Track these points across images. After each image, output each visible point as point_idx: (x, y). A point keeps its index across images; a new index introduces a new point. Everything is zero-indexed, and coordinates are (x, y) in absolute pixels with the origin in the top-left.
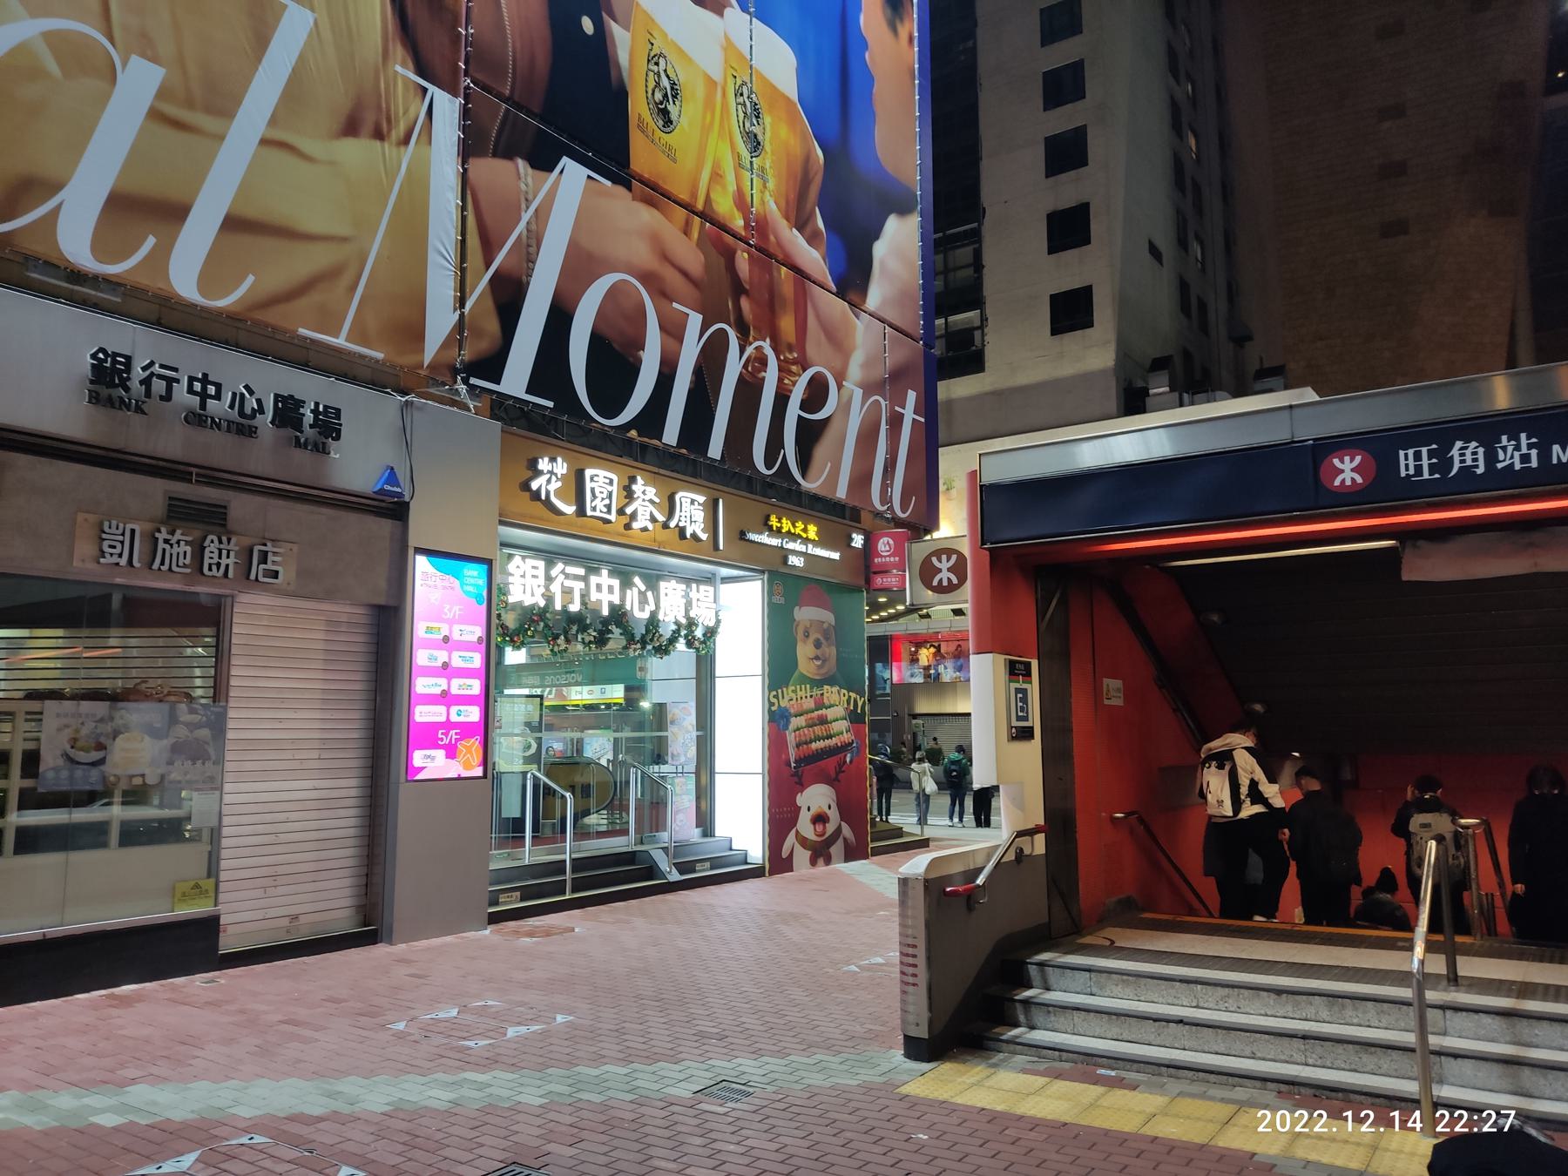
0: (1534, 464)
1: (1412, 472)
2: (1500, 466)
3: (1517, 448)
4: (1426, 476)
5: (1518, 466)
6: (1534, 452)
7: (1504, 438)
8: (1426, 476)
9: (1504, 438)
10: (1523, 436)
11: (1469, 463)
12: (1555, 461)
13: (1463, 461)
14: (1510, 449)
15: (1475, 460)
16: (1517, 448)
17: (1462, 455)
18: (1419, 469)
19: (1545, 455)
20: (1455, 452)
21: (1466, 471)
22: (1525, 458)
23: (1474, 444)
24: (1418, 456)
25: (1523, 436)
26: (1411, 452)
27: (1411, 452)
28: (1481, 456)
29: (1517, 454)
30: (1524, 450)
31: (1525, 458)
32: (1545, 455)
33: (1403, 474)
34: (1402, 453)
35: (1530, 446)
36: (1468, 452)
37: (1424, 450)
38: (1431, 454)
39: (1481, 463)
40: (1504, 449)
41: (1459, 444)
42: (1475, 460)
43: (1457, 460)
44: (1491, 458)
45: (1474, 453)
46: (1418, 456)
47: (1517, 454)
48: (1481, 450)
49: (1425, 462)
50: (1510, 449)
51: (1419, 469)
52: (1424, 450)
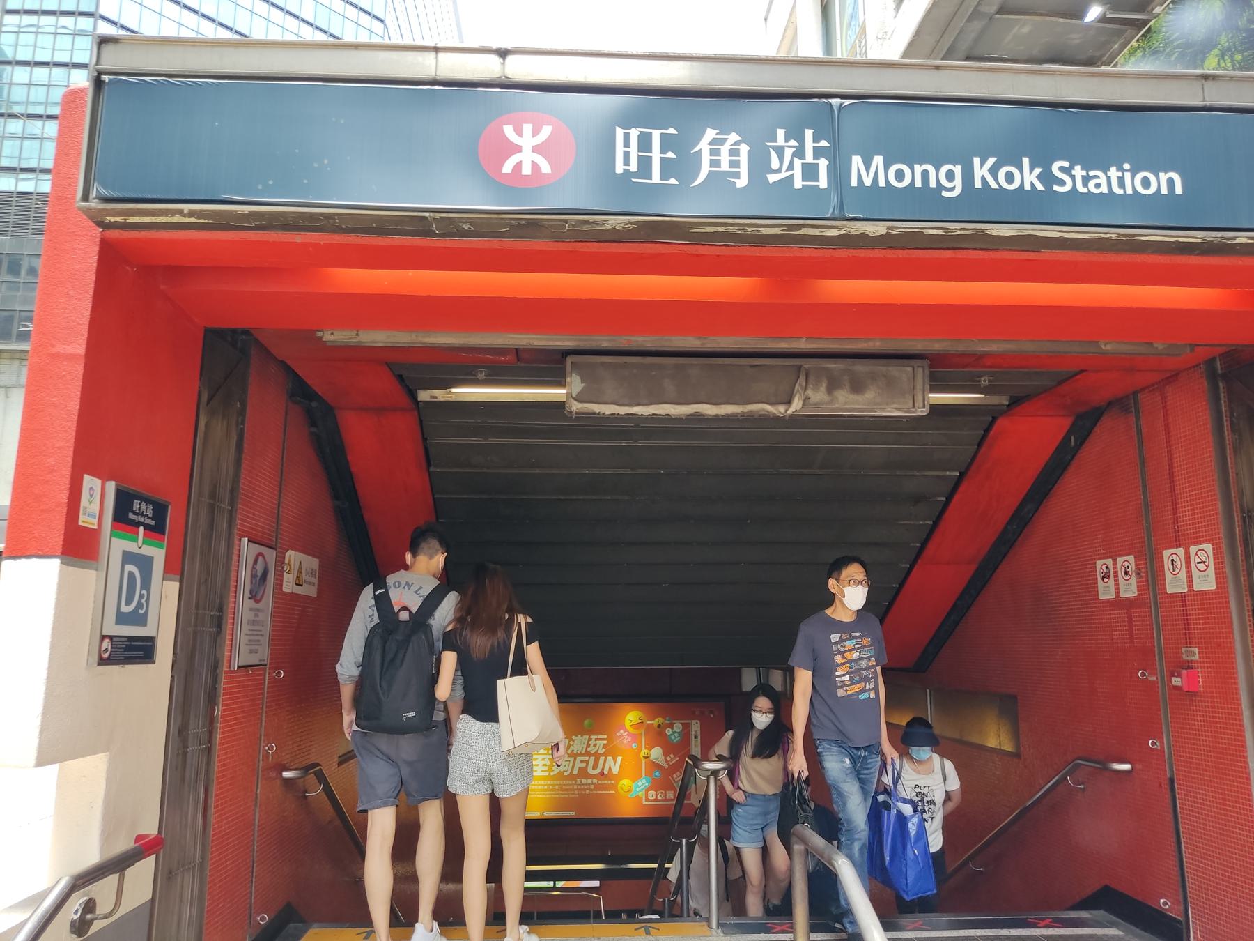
0: (823, 183)
1: (633, 167)
2: (772, 178)
5: (798, 183)
6: (823, 164)
7: (781, 133)
8: (656, 178)
9: (781, 133)
10: (809, 133)
11: (725, 166)
12: (854, 183)
14: (788, 153)
17: (715, 152)
18: (645, 164)
19: (839, 172)
20: (704, 146)
22: (810, 172)
23: (734, 137)
25: (809, 133)
26: (634, 133)
27: (634, 133)
28: (743, 159)
29: (798, 163)
30: (809, 158)
31: (810, 172)
32: (839, 172)
33: (619, 168)
34: (620, 132)
35: (818, 153)
36: (725, 149)
38: (666, 143)
39: (744, 169)
40: (780, 151)
41: (710, 134)
44: (759, 165)
45: (734, 152)
47: (798, 163)
48: (744, 149)
49: (656, 155)
50: (788, 153)
51: (645, 164)
52: (656, 135)
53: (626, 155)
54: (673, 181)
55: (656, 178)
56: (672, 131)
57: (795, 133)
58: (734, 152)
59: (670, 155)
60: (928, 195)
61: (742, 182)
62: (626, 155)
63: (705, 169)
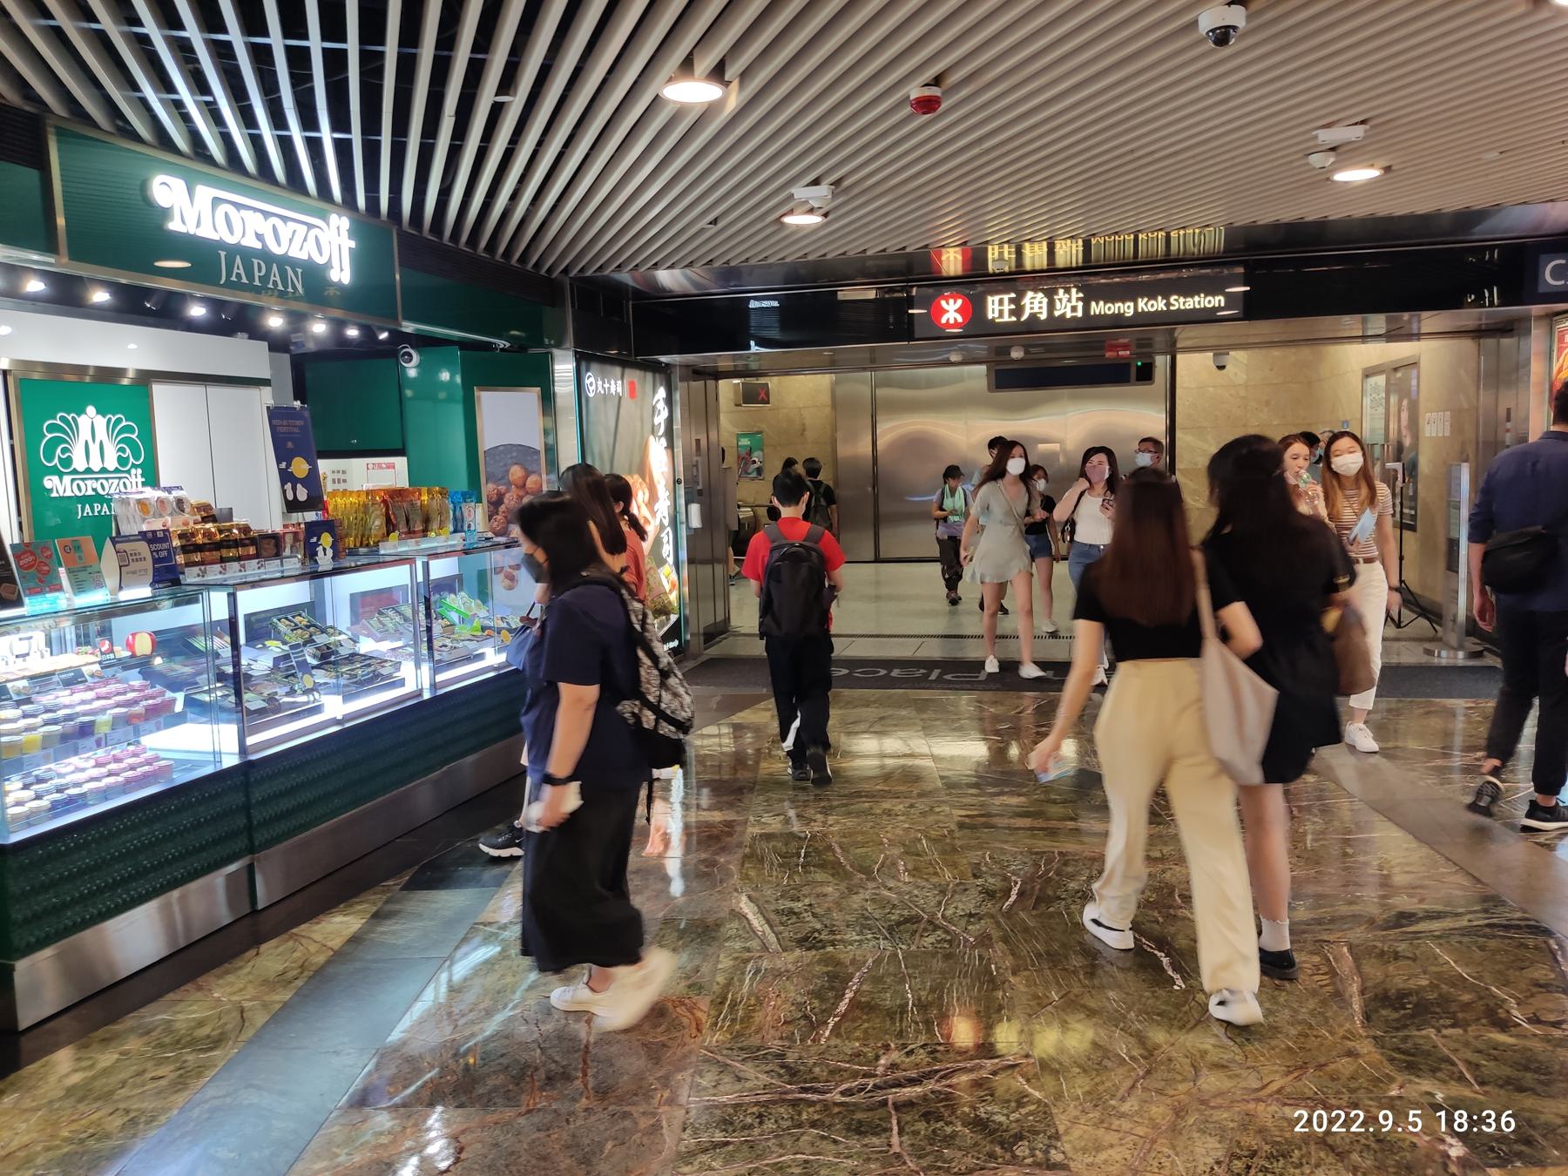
2: (1057, 314)
3: (1069, 300)
4: (1006, 318)
6: (1080, 305)
11: (1036, 310)
16: (1069, 300)
18: (1001, 312)
20: (1026, 301)
21: (1033, 316)
22: (1074, 309)
24: (1001, 302)
26: (996, 298)
30: (1074, 303)
32: (1086, 308)
33: (990, 316)
34: (990, 299)
37: (1006, 297)
38: (1011, 301)
46: (1001, 302)
48: (1045, 300)
51: (1001, 312)
56: (1013, 295)
57: (1067, 291)
60: (1120, 316)
61: (1043, 316)
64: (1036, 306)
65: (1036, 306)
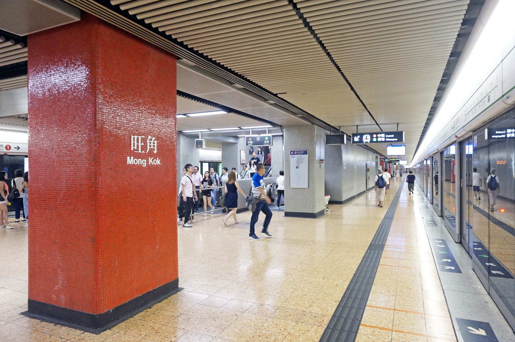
1: (136, 148)
4: (140, 151)
11: (152, 147)
13: (150, 146)
15: (154, 146)
17: (150, 143)
18: (138, 145)
23: (154, 138)
26: (136, 137)
28: (156, 145)
36: (152, 142)
37: (140, 137)
39: (156, 148)
42: (154, 146)
43: (148, 144)
45: (154, 143)
48: (156, 142)
49: (140, 144)
51: (138, 145)
53: (134, 143)
54: (143, 152)
55: (140, 151)
56: (143, 137)
58: (154, 143)
59: (143, 144)
62: (134, 143)
63: (148, 148)
64: (152, 144)
65: (152, 144)
